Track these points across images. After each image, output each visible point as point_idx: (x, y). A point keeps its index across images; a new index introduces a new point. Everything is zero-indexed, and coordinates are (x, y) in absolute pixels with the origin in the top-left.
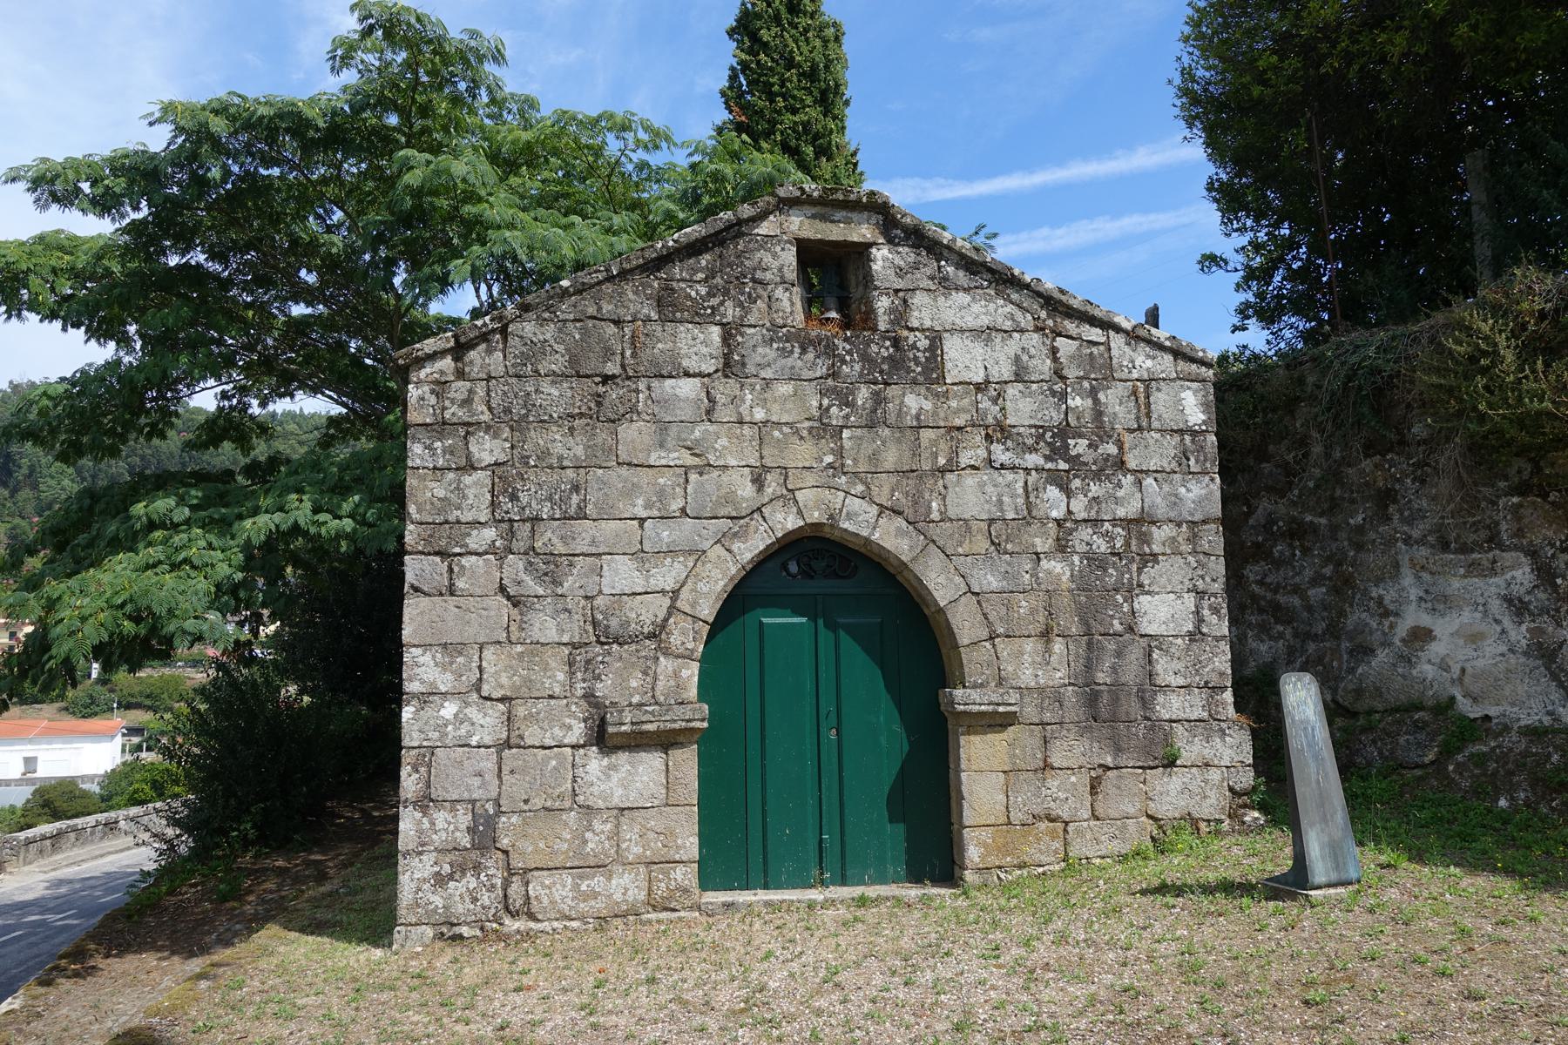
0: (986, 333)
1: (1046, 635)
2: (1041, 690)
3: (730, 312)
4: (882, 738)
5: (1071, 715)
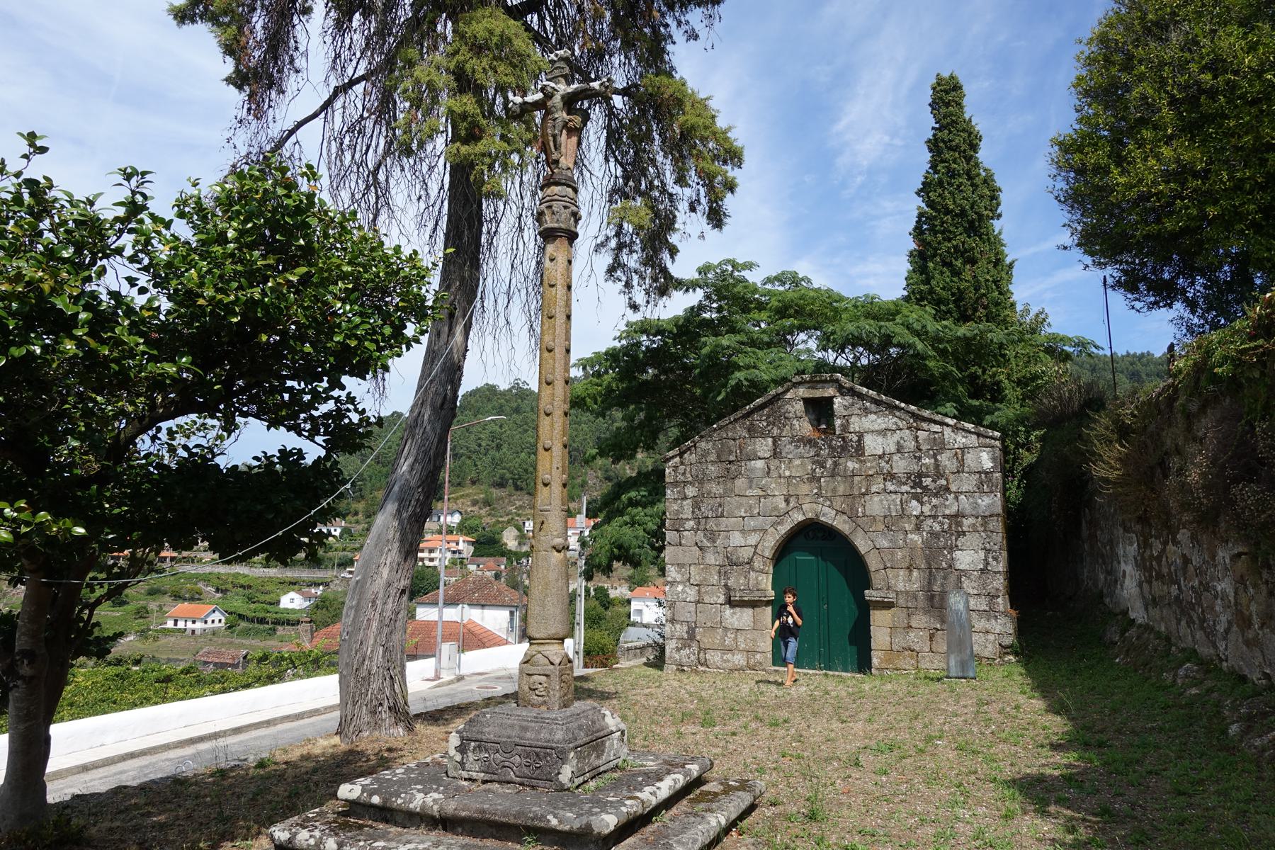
0: (883, 432)
1: (909, 568)
2: (907, 592)
3: (776, 431)
4: (850, 611)
5: (920, 605)
